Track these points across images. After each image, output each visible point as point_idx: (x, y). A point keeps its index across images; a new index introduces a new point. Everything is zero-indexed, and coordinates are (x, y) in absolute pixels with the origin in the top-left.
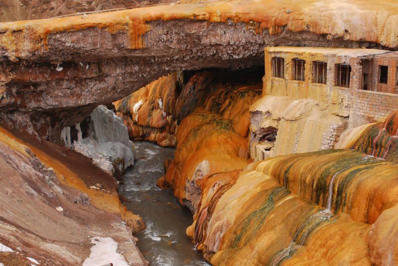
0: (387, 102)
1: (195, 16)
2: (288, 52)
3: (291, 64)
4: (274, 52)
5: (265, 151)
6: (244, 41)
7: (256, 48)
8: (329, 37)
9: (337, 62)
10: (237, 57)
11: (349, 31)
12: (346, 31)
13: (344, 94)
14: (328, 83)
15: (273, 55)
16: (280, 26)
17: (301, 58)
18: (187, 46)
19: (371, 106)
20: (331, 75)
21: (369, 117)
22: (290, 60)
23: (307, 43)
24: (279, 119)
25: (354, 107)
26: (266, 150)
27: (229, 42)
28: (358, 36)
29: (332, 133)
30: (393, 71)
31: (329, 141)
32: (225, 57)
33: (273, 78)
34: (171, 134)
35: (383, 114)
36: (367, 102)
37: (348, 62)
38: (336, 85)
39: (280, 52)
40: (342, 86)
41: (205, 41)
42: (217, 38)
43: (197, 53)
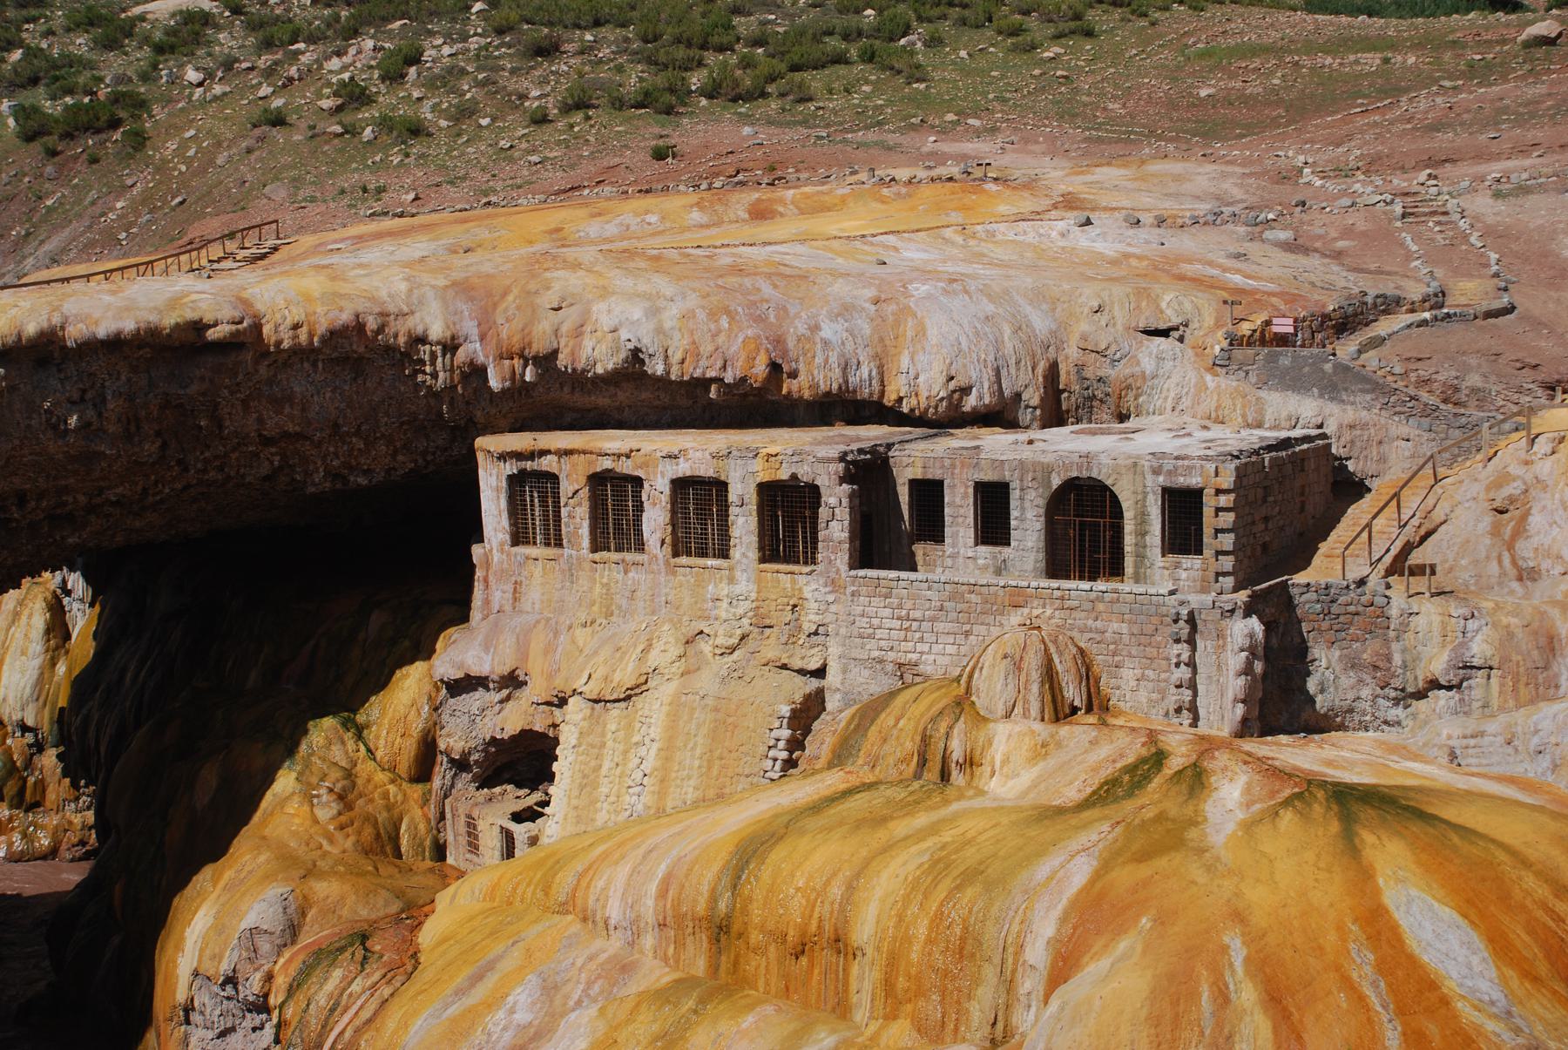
0: (960, 607)
1: (199, 327)
3: (585, 493)
4: (518, 456)
5: (513, 826)
7: (440, 442)
9: (764, 477)
10: (363, 481)
14: (736, 553)
15: (511, 468)
17: (625, 467)
18: (164, 446)
19: (906, 624)
20: (744, 526)
21: (900, 665)
22: (583, 480)
24: (563, 702)
25: (843, 631)
26: (518, 817)
27: (336, 426)
29: (775, 734)
30: (965, 496)
32: (318, 481)
34: (27, 811)
35: (950, 649)
36: (888, 612)
37: (805, 473)
38: (763, 560)
39: (544, 453)
40: (790, 558)
42: (287, 410)
43: (205, 471)
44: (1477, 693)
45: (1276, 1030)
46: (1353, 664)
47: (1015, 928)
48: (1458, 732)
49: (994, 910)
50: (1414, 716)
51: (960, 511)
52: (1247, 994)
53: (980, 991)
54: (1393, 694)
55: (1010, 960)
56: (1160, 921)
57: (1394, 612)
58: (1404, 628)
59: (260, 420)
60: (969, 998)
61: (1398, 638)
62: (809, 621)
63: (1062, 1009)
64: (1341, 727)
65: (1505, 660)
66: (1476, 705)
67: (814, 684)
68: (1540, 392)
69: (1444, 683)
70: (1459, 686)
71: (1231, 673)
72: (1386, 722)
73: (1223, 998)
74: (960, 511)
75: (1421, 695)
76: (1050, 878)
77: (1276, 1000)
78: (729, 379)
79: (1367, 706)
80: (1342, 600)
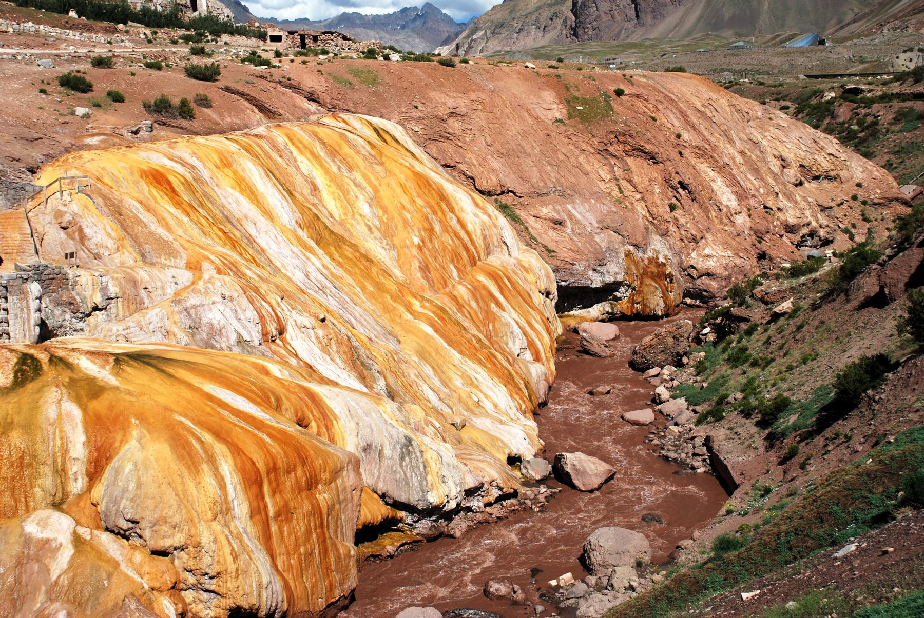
44: (113, 311)
45: (230, 449)
46: (58, 304)
47: (58, 443)
48: (121, 328)
49: (39, 438)
50: (88, 325)
52: (207, 437)
53: (40, 481)
54: (81, 315)
55: (59, 460)
56: (141, 417)
57: (71, 276)
58: (75, 283)
60: (32, 487)
61: (73, 289)
63: (136, 465)
64: (56, 336)
65: (124, 293)
66: (113, 316)
68: (28, 173)
69: (100, 307)
70: (105, 309)
71: (32, 311)
72: (76, 330)
73: (202, 442)
75: (89, 315)
76: (60, 415)
77: (218, 435)
79: (67, 323)
80: (45, 272)
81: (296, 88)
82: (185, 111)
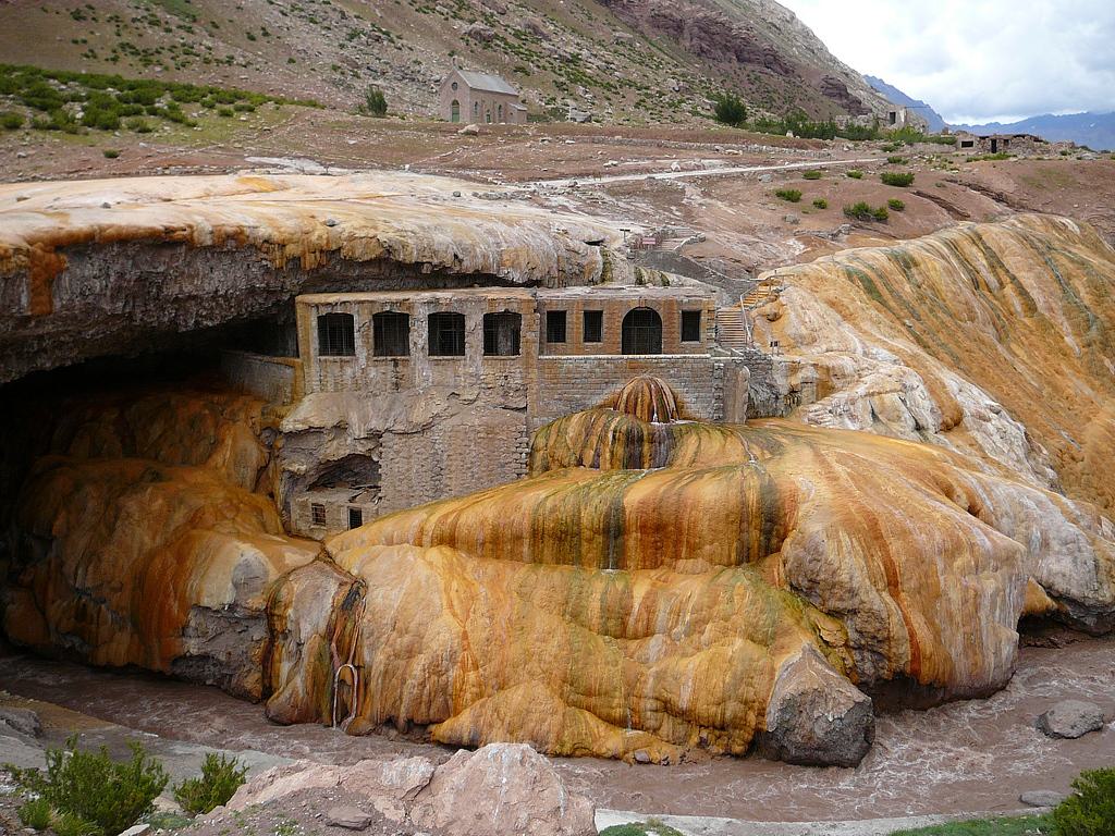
2: (362, 304)
6: (242, 285)
8: (426, 270)
10: (210, 324)
11: (460, 256)
12: (456, 256)
13: (514, 370)
15: (324, 311)
16: (331, 253)
20: (475, 338)
23: (361, 284)
27: (217, 291)
28: (469, 265)
30: (578, 318)
31: (515, 456)
33: (323, 358)
37: (514, 308)
41: (172, 290)
51: (575, 325)
59: (181, 288)
62: (516, 381)
67: (523, 416)
74: (575, 325)
78: (436, 261)
81: (985, 191)
82: (881, 218)
